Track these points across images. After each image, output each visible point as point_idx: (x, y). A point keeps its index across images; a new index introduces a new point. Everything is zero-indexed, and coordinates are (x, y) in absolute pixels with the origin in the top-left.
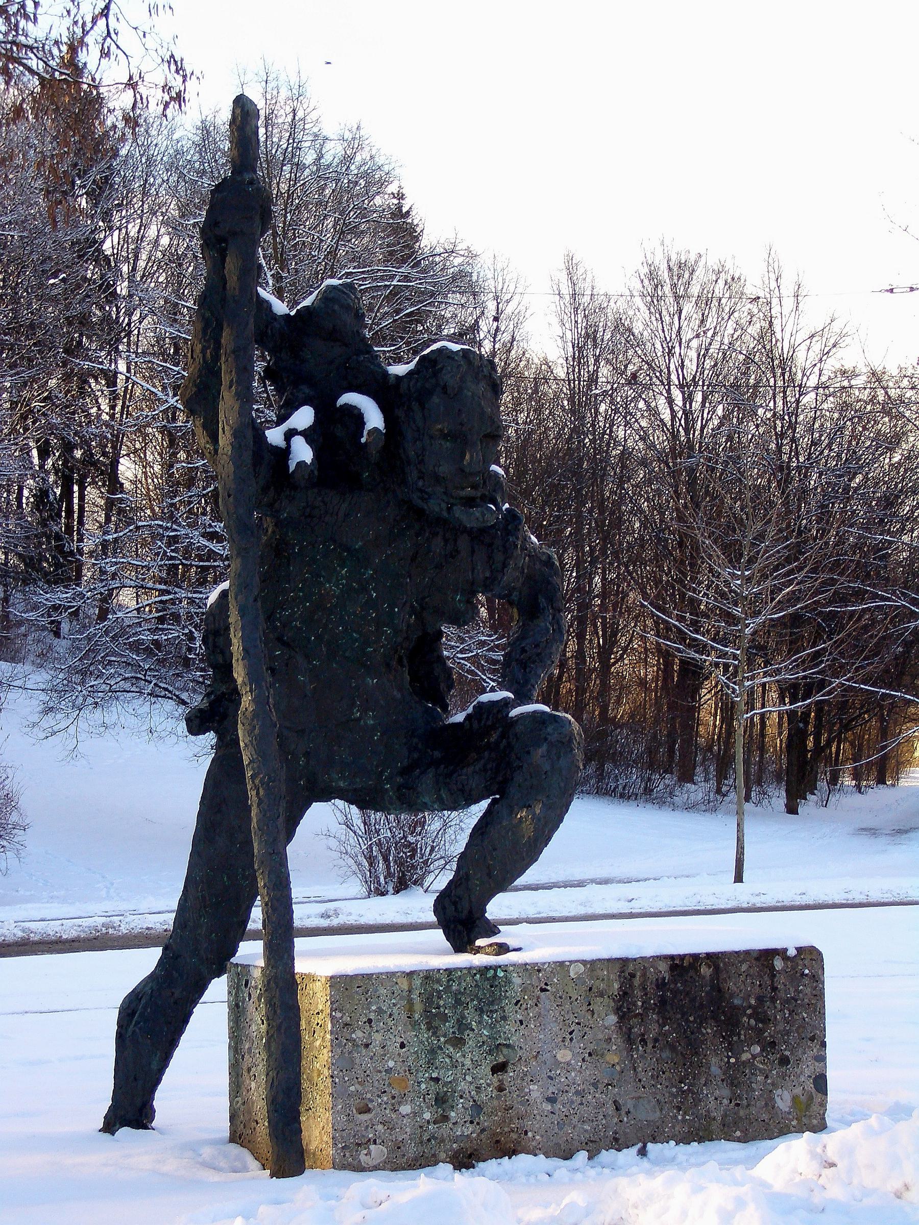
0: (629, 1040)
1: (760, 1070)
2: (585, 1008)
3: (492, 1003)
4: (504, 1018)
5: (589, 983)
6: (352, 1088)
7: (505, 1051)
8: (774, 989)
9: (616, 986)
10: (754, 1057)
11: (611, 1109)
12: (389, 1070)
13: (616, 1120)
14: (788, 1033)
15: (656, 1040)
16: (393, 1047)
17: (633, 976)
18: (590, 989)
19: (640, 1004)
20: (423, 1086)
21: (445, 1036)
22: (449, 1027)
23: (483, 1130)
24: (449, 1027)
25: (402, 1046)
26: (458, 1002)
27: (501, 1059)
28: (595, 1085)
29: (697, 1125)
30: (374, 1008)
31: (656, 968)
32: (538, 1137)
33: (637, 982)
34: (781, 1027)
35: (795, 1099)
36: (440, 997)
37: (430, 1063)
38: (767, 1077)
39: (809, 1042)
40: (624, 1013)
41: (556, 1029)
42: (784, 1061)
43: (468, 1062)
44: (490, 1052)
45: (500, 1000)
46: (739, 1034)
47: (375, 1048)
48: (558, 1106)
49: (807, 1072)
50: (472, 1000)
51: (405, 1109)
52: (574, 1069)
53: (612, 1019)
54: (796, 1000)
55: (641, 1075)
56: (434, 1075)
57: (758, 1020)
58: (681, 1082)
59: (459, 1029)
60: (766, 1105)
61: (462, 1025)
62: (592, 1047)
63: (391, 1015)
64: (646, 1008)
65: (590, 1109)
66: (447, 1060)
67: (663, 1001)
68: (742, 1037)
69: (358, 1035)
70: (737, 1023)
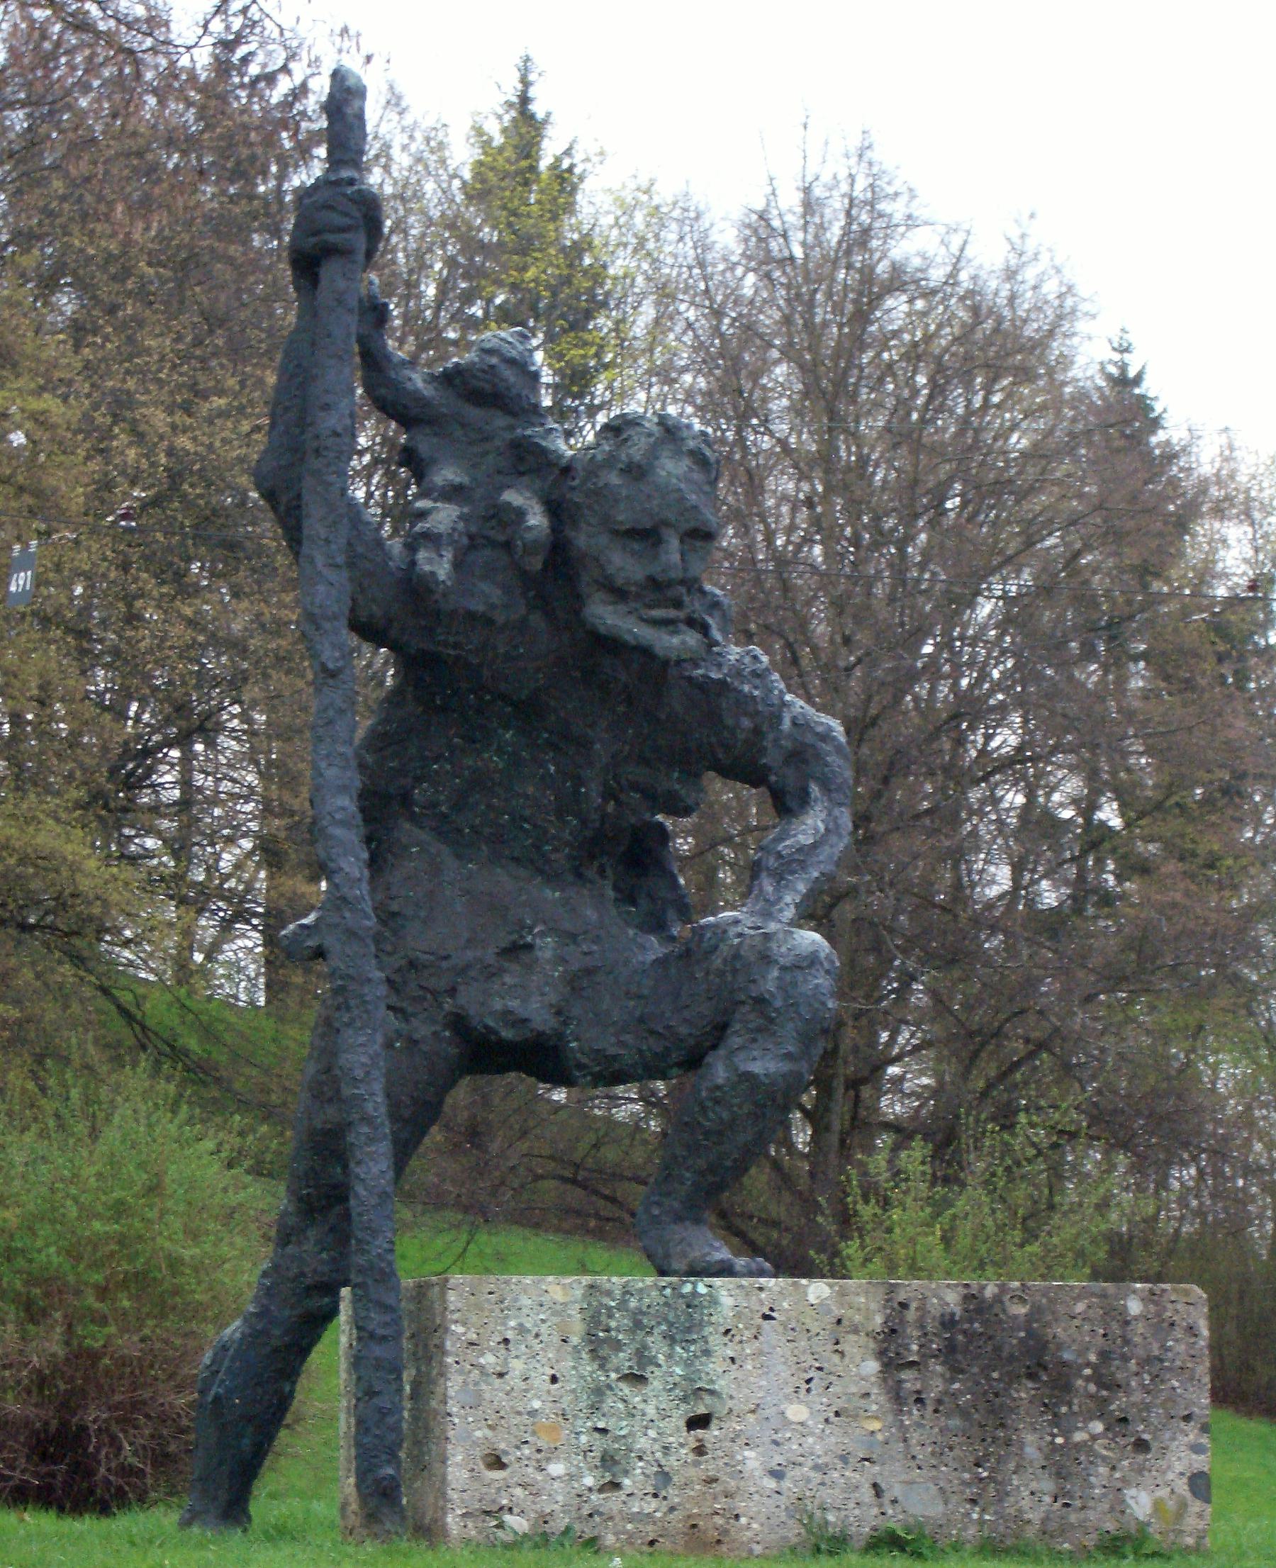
0: (897, 1397)
1: (1104, 1458)
2: (831, 1347)
3: (689, 1330)
4: (707, 1353)
5: (838, 1312)
6: (478, 1434)
7: (708, 1399)
8: (1127, 1342)
9: (879, 1319)
10: (1094, 1438)
11: (867, 1494)
12: (533, 1413)
13: (875, 1511)
14: (1148, 1407)
15: (939, 1402)
16: (540, 1381)
17: (904, 1306)
18: (839, 1322)
19: (915, 1347)
20: (584, 1439)
21: (617, 1370)
22: (623, 1360)
23: (672, 1509)
24: (623, 1360)
25: (554, 1379)
26: (638, 1325)
27: (702, 1410)
28: (844, 1459)
29: (1001, 1529)
30: (512, 1323)
31: (940, 1299)
32: (755, 1526)
33: (911, 1315)
34: (1137, 1397)
35: (1158, 1505)
36: (610, 1316)
37: (595, 1408)
38: (1114, 1468)
39: (1182, 1424)
40: (892, 1363)
41: (785, 1374)
42: (1142, 1446)
43: (651, 1411)
44: (684, 1399)
45: (701, 1325)
46: (1070, 1404)
47: (514, 1380)
48: (787, 1484)
49: (1179, 1467)
50: (659, 1324)
51: (557, 1469)
52: (812, 1434)
53: (872, 1366)
54: (1161, 1361)
55: (916, 1450)
56: (601, 1425)
57: (1101, 1385)
58: (978, 1465)
59: (639, 1364)
60: (1112, 1509)
61: (643, 1357)
62: (839, 1404)
63: (537, 1336)
64: (925, 1354)
65: (837, 1491)
66: (621, 1405)
67: (950, 1349)
68: (1075, 1408)
69: (488, 1360)
70: (1067, 1388)
